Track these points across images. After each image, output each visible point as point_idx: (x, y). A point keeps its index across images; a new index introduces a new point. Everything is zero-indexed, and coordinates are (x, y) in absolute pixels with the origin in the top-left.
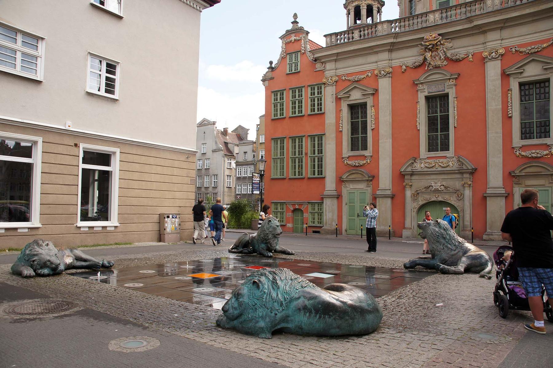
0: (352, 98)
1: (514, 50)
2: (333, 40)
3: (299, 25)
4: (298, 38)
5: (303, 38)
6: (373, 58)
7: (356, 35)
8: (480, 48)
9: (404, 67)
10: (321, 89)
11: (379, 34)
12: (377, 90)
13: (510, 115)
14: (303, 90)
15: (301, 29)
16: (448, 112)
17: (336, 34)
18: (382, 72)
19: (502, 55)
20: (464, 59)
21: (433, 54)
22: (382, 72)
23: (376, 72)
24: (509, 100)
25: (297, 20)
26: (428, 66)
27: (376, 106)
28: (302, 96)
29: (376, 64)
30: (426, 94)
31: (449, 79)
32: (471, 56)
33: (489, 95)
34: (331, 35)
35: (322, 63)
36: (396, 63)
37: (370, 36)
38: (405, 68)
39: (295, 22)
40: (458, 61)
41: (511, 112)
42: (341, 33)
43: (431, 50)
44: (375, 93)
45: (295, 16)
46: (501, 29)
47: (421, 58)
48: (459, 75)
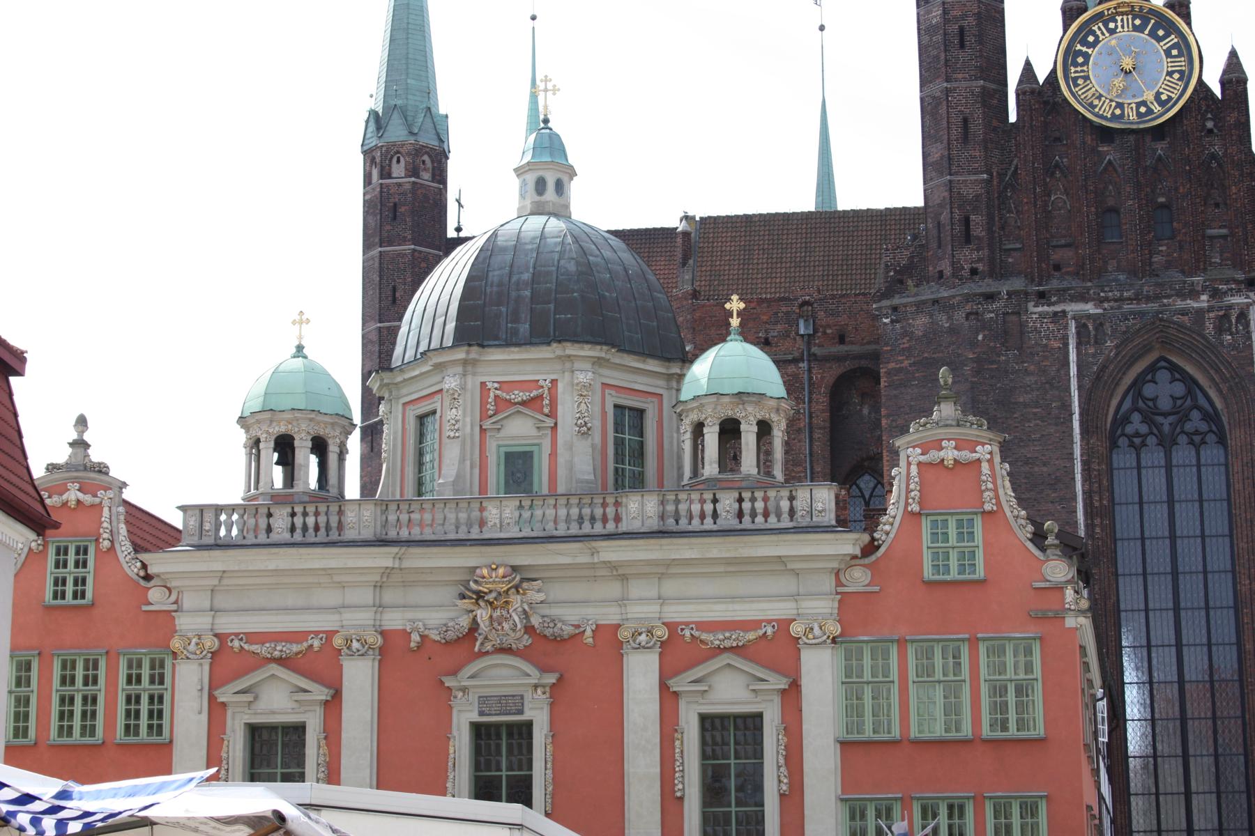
0: (262, 705)
1: (687, 633)
2: (207, 526)
3: (95, 455)
4: (87, 499)
5: (106, 503)
6: (332, 598)
7: (281, 521)
8: (610, 615)
9: (415, 637)
10: (162, 666)
11: (349, 534)
12: (337, 695)
13: (679, 794)
14: (102, 664)
15: (102, 469)
16: (530, 768)
17: (218, 509)
18: (355, 645)
19: (662, 642)
20: (573, 637)
21: (495, 615)
22: (355, 645)
23: (338, 641)
24: (677, 756)
25: (86, 437)
26: (482, 644)
27: (332, 735)
28: (95, 682)
29: (336, 617)
30: (476, 717)
31: (536, 687)
32: (589, 633)
33: (630, 738)
34: (201, 509)
35: (169, 589)
36: (394, 620)
37: (322, 535)
38: (418, 639)
39: (80, 445)
40: (558, 640)
41: (680, 786)
42: (232, 509)
43: (491, 603)
44: (333, 705)
45: (82, 422)
46: (661, 577)
47: (465, 622)
48: (560, 680)
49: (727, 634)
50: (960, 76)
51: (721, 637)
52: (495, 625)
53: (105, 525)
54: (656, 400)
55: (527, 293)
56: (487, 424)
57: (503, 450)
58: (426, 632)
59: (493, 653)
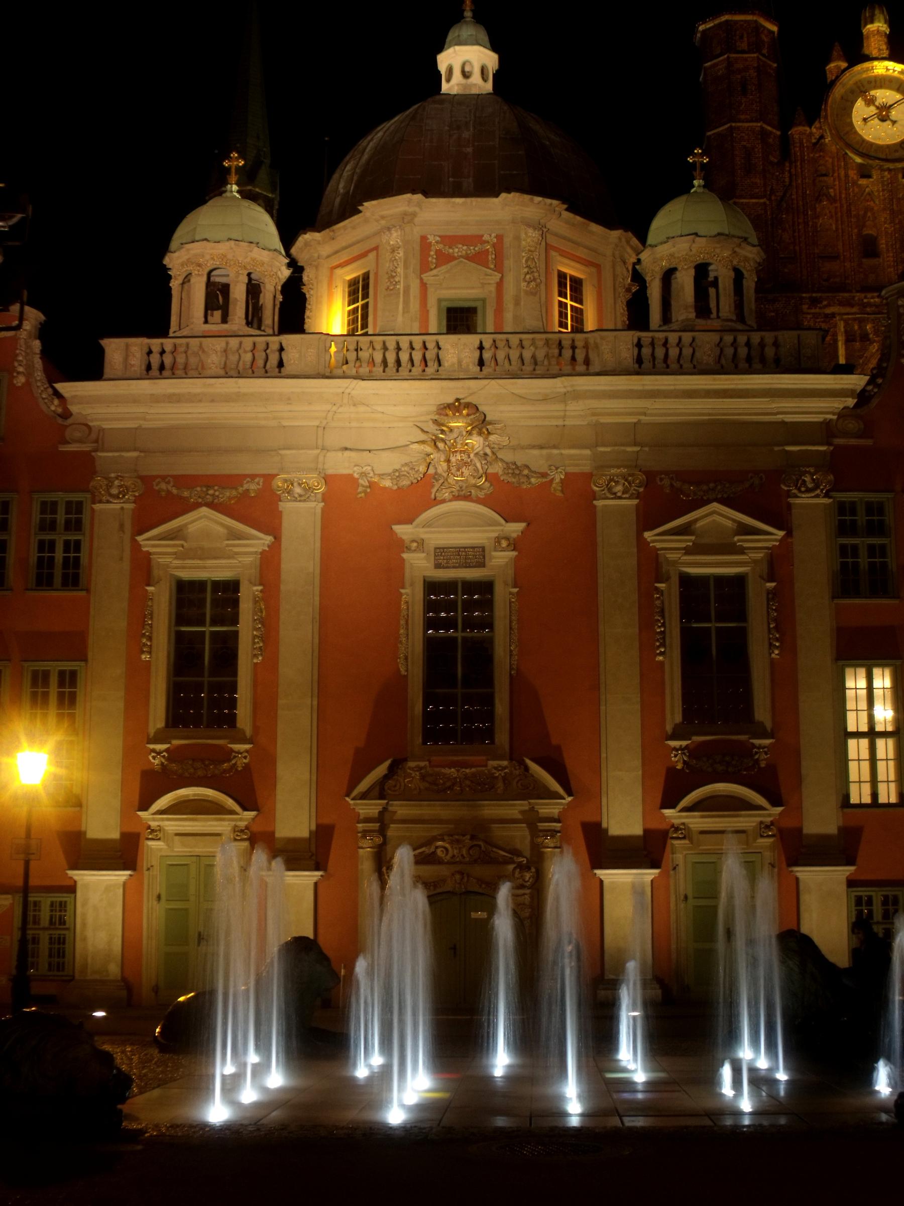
1: (667, 482)
18: (298, 490)
49: (712, 485)
50: (743, 117)
51: (705, 487)
52: (454, 470)
53: (20, 358)
54: (594, 270)
55: (470, 150)
56: (427, 277)
57: (446, 304)
58: (376, 480)
59: (450, 501)
